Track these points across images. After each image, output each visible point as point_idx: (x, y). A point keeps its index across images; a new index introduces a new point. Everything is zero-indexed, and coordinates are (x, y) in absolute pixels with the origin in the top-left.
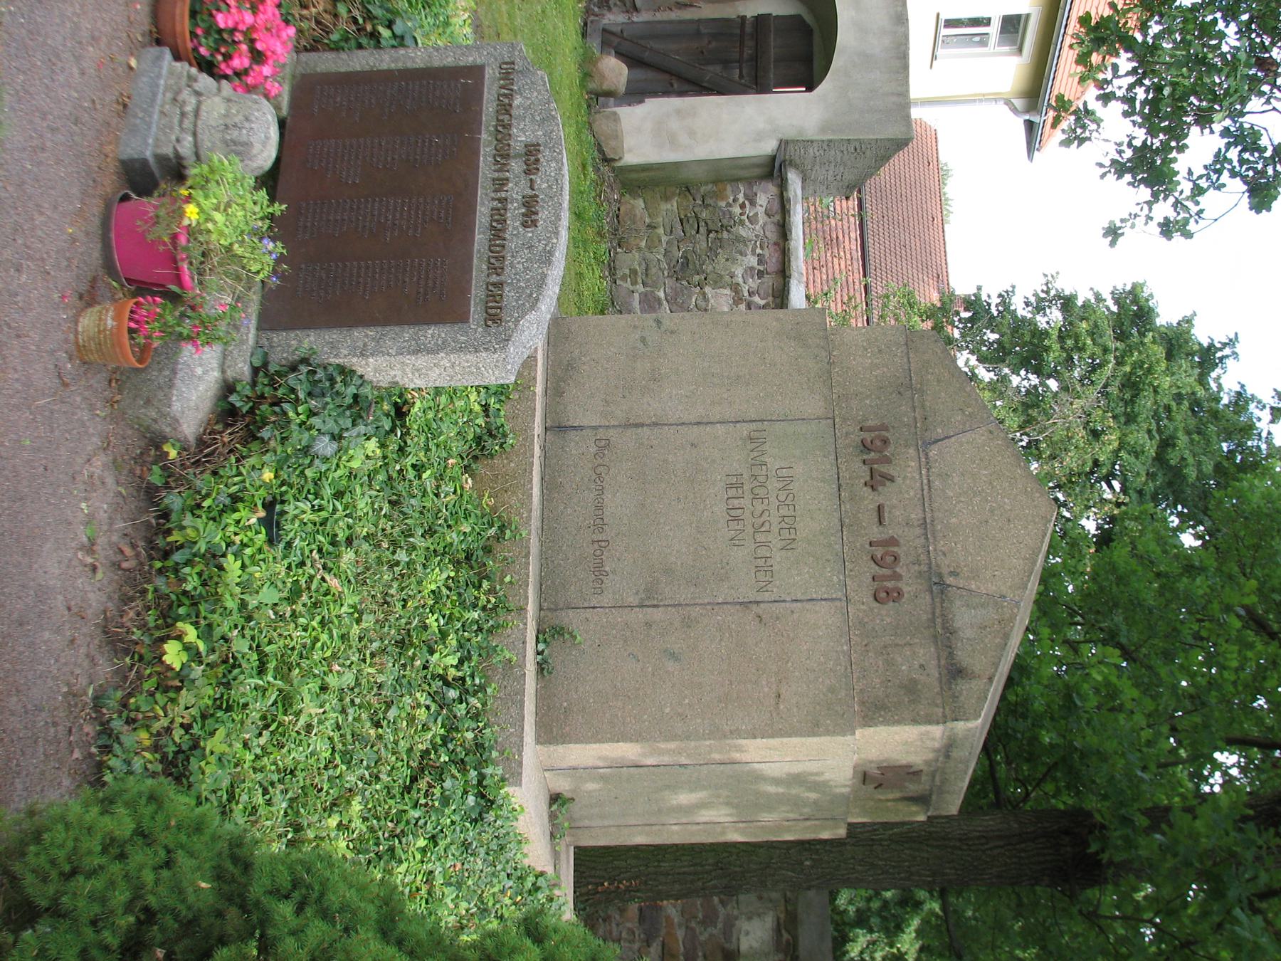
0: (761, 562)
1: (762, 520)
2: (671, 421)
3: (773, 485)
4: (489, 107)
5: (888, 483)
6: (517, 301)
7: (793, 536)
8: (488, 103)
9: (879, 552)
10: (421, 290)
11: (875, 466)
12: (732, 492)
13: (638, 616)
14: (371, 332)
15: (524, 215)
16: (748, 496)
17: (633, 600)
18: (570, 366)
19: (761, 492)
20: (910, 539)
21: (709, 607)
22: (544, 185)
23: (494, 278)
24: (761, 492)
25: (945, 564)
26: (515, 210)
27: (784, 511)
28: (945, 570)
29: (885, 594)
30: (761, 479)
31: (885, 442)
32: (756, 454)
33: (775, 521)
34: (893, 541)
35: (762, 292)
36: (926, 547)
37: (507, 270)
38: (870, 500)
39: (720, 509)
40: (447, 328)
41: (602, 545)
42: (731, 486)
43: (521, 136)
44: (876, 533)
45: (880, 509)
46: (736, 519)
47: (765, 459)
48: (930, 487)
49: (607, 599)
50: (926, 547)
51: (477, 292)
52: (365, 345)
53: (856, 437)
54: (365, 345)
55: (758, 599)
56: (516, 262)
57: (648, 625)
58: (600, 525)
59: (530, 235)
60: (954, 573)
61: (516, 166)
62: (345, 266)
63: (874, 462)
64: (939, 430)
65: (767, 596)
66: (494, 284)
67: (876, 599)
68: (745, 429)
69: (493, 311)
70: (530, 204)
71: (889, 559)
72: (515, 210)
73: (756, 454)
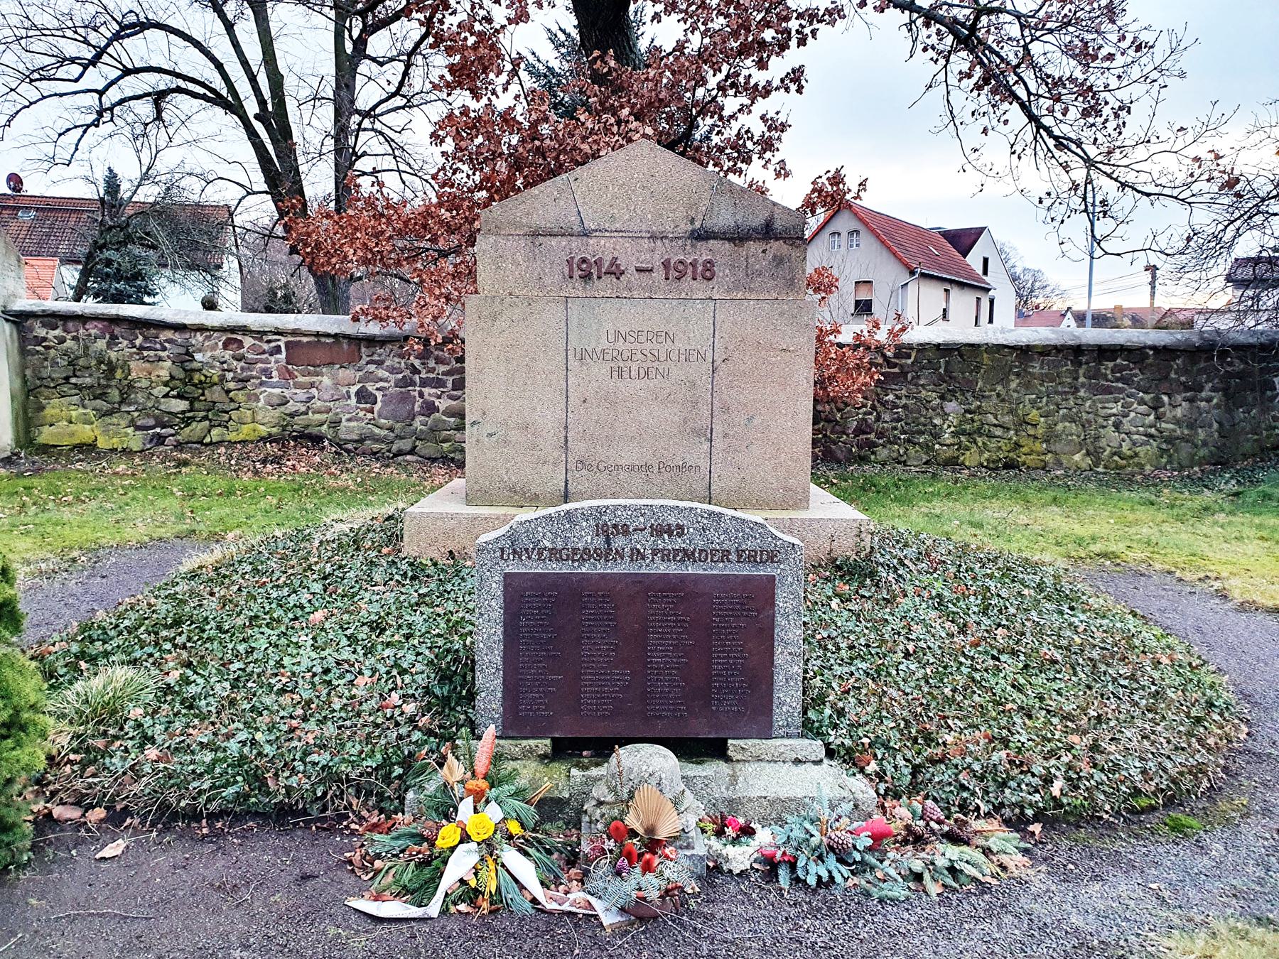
0: (683, 357)
1: (649, 355)
2: (564, 417)
3: (620, 345)
4: (553, 567)
5: (618, 262)
6: (756, 539)
7: (663, 334)
8: (547, 568)
9: (673, 274)
10: (745, 613)
11: (603, 270)
12: (626, 375)
13: (718, 443)
14: (778, 650)
15: (670, 536)
16: (629, 363)
17: (706, 446)
18: (512, 490)
19: (626, 355)
20: (662, 251)
21: (715, 394)
22: (641, 519)
23: (733, 557)
24: (626, 355)
25: (685, 227)
26: (665, 543)
27: (643, 339)
28: (690, 228)
29: (708, 272)
30: (615, 353)
31: (584, 260)
32: (595, 356)
33: (648, 346)
34: (666, 265)
35: (131, 338)
36: (672, 240)
37: (725, 547)
38: (631, 276)
39: (637, 384)
40: (778, 592)
41: (662, 466)
42: (621, 376)
43: (586, 537)
44: (659, 275)
45: (639, 270)
46: (647, 373)
47: (598, 350)
48: (621, 231)
49: (704, 464)
50: (672, 240)
51: (746, 570)
52: (790, 654)
53: (579, 284)
54: (790, 654)
55: (711, 360)
56: (718, 539)
57: (725, 436)
58: (646, 468)
59: (691, 530)
60: (692, 221)
61: (619, 542)
62: (716, 675)
63: (599, 270)
64: (573, 218)
65: (709, 355)
66: (740, 556)
67: (710, 279)
68: (573, 364)
69: (765, 557)
70: (659, 531)
71: (681, 267)
72: (665, 543)
73: (595, 356)
